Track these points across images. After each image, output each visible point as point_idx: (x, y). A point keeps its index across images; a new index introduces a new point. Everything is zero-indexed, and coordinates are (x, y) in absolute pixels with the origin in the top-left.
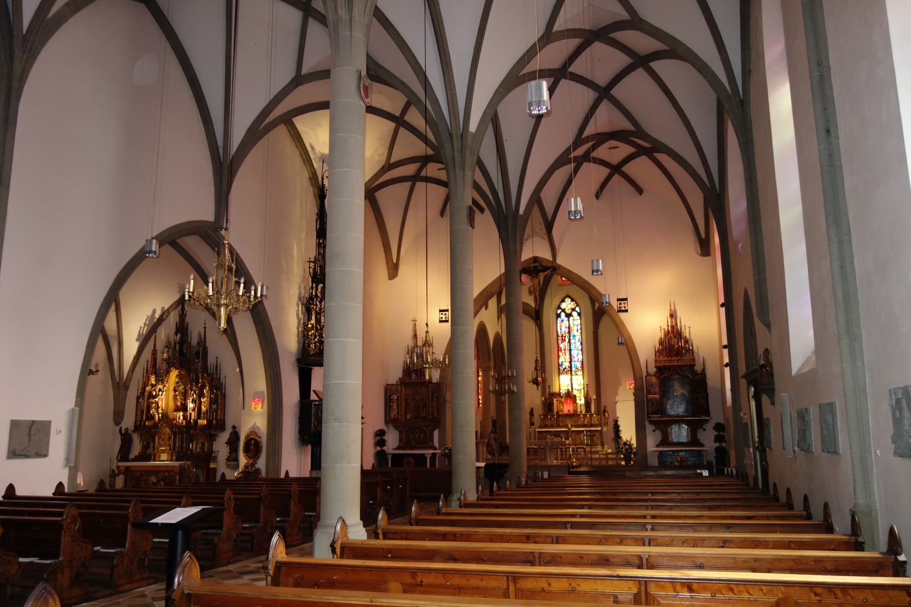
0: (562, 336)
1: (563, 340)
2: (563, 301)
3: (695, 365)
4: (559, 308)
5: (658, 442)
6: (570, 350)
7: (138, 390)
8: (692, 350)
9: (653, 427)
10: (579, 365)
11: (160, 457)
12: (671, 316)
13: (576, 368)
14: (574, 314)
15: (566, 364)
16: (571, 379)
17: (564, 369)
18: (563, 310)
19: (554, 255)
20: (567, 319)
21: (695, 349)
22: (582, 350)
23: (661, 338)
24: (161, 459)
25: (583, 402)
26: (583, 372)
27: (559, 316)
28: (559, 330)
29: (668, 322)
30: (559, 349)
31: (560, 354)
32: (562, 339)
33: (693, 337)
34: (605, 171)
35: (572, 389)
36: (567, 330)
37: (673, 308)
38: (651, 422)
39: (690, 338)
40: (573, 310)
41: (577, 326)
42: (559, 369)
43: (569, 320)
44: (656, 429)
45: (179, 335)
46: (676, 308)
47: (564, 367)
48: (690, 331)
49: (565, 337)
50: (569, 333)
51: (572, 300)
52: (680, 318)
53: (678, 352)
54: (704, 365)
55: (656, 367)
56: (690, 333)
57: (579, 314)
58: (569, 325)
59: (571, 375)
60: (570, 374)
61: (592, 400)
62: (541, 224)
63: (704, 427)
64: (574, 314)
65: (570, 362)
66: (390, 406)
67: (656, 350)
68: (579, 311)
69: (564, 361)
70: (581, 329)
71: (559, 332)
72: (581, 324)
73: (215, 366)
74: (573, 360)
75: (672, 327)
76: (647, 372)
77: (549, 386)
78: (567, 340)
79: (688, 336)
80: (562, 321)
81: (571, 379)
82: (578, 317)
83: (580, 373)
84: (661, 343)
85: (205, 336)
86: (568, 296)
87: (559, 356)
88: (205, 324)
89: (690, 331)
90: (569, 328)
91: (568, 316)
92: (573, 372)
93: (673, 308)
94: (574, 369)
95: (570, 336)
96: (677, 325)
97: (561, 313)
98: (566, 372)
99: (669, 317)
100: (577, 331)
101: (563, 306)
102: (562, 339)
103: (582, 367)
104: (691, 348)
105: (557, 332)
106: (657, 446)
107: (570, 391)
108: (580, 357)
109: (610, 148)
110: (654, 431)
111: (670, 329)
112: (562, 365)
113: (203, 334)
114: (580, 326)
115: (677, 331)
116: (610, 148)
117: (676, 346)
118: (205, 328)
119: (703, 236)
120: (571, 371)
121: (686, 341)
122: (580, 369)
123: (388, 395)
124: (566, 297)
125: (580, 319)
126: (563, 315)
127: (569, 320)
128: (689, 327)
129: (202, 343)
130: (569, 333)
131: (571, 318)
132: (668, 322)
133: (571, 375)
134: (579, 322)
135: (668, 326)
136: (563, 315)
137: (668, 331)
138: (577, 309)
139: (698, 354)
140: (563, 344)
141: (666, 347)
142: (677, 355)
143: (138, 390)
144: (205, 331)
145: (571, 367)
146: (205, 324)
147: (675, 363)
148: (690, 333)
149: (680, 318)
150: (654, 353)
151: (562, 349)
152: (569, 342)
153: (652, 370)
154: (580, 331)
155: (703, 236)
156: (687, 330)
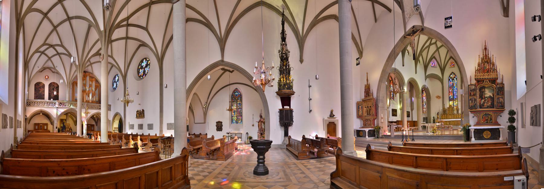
2: (451, 74)
6: (453, 92)
16: (453, 102)
18: (451, 78)
58: (453, 83)
59: (453, 101)
65: (453, 97)
66: (359, 111)
81: (453, 102)
91: (453, 80)
101: (451, 76)
126: (451, 79)
133: (453, 101)
136: (451, 79)
142: (488, 72)
145: (453, 98)
152: (453, 88)
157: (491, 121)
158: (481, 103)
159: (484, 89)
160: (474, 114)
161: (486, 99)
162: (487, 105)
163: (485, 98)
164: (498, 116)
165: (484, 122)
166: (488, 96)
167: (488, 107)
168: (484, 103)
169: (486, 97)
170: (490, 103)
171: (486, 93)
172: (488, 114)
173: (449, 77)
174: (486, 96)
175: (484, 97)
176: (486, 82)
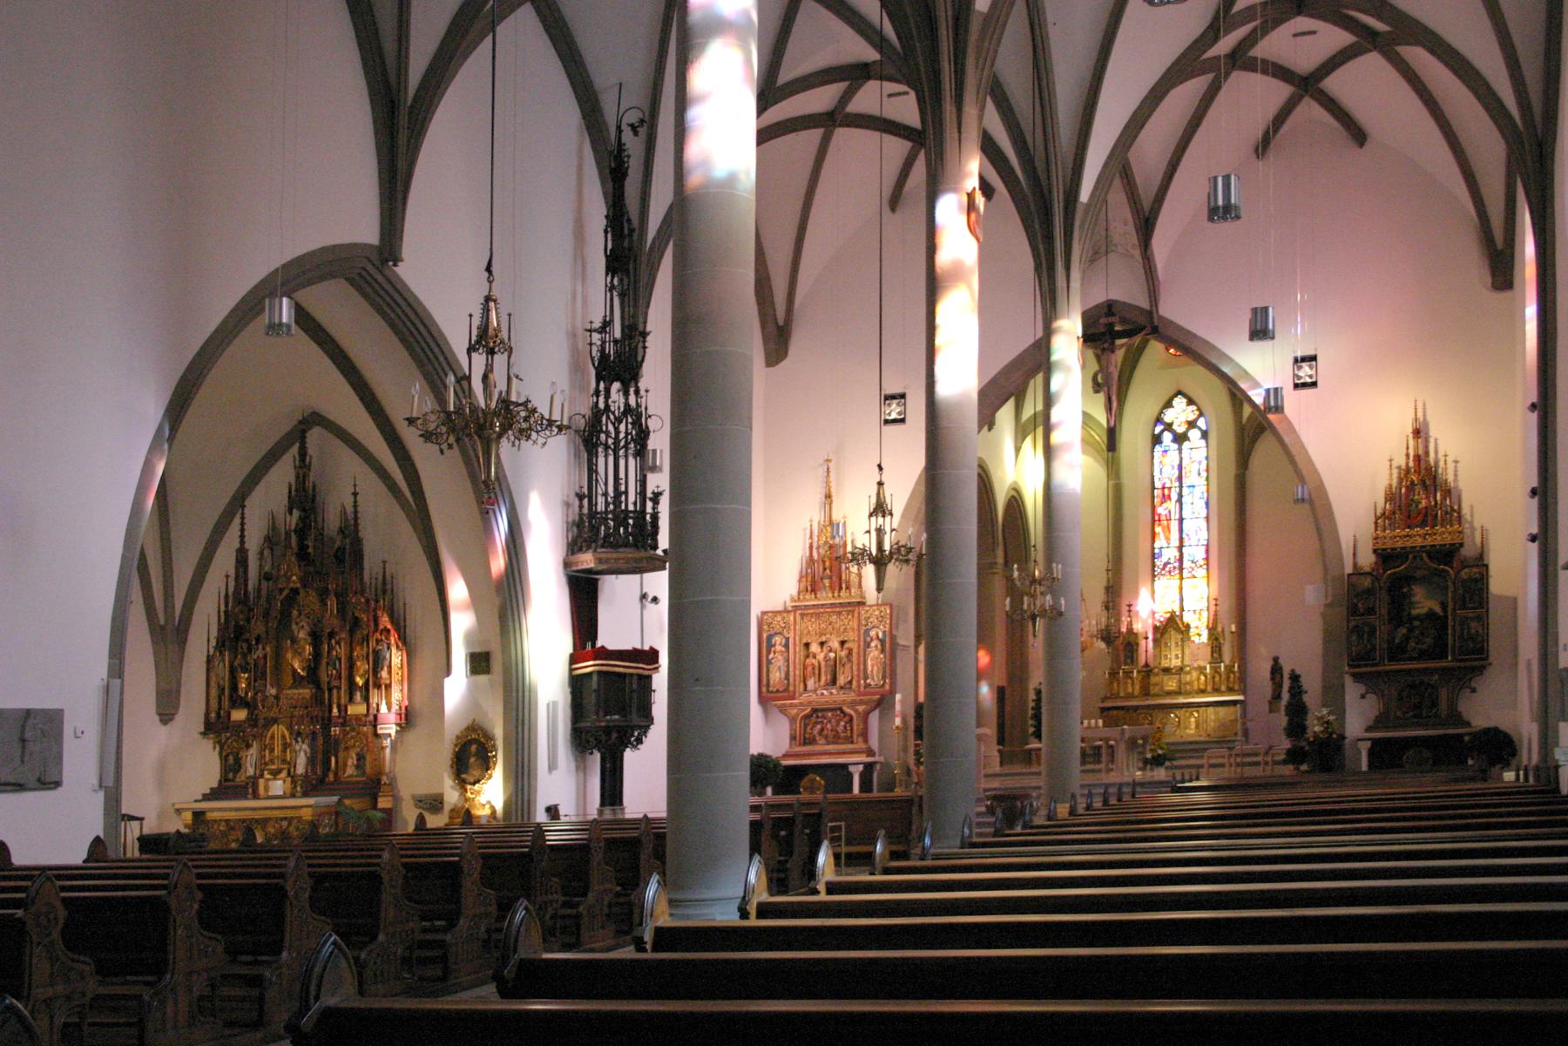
0: (1164, 488)
1: (1165, 498)
3: (1462, 545)
4: (1159, 420)
5: (1371, 723)
7: (208, 641)
8: (1459, 512)
9: (1361, 688)
10: (1200, 554)
11: (267, 789)
12: (1417, 433)
13: (1193, 562)
14: (1194, 434)
15: (1170, 554)
16: (1181, 588)
17: (1166, 564)
18: (1169, 427)
19: (1153, 293)
20: (1175, 446)
21: (1466, 510)
22: (1207, 518)
23: (1391, 486)
24: (270, 794)
25: (1205, 638)
26: (1208, 569)
27: (1157, 440)
28: (1156, 474)
29: (1408, 448)
30: (1155, 519)
31: (1158, 529)
32: (1164, 495)
33: (1461, 485)
34: (1280, 92)
35: (1182, 609)
36: (1176, 473)
37: (1420, 415)
38: (1357, 677)
39: (1456, 487)
40: (1192, 424)
41: (1200, 462)
42: (1154, 565)
43: (1180, 450)
44: (1366, 693)
45: (296, 513)
46: (1428, 418)
47: (1164, 559)
48: (1456, 471)
49: (1170, 488)
50: (1180, 478)
51: (1191, 402)
52: (1436, 440)
53: (1426, 515)
54: (1483, 547)
55: (1375, 551)
56: (1456, 475)
57: (1205, 435)
58: (1181, 459)
59: (1182, 578)
60: (1178, 576)
61: (1227, 633)
62: (1126, 224)
63: (1473, 684)
64: (1194, 434)
67: (1378, 514)
68: (1204, 428)
69: (1165, 545)
70: (1207, 470)
71: (1156, 480)
72: (1207, 458)
73: (380, 578)
74: (1186, 542)
75: (1418, 458)
76: (1355, 565)
77: (1130, 606)
78: (1174, 496)
79: (1450, 478)
80: (1165, 451)
81: (1181, 588)
82: (1203, 443)
83: (1202, 572)
84: (1390, 497)
85: (356, 512)
86: (1179, 393)
87: (1154, 535)
88: (355, 486)
89: (1456, 471)
90: (1180, 467)
91: (1180, 439)
92: (1185, 572)
93: (1420, 415)
94: (1186, 564)
95: (1181, 487)
96: (1427, 453)
97: (1162, 432)
98: (1170, 572)
99: (1411, 436)
100: (1199, 474)
101: (1168, 416)
102: (1164, 495)
103: (1207, 559)
104: (1456, 507)
105: (1153, 477)
106: (1369, 729)
107: (1178, 613)
108: (1204, 535)
109: (1295, 35)
110: (1363, 697)
111: (1411, 464)
112: (1160, 555)
113: (350, 509)
114: (1205, 463)
115: (1428, 469)
116: (1295, 35)
117: (1424, 501)
118: (355, 494)
119: (1500, 243)
120: (1181, 569)
121: (1448, 492)
122: (1202, 562)
123: (765, 636)
124: (1176, 395)
125: (1207, 447)
126: (1167, 437)
127: (1180, 450)
128: (1456, 462)
129: (351, 529)
130: (1180, 478)
131: (1186, 445)
132: (1408, 448)
133: (1182, 578)
134: (1203, 453)
135: (1408, 455)
136: (1167, 437)
137: (1408, 470)
138: (1201, 423)
139: (1471, 523)
140: (1164, 505)
141: (1400, 506)
142: (1423, 524)
143: (208, 641)
144: (355, 502)
145: (1181, 560)
146: (355, 486)
147: (1419, 542)
148: (1456, 475)
149: (1436, 440)
150: (1373, 520)
151: (1163, 518)
153: (1367, 559)
154: (1204, 474)
155: (1500, 243)
156: (1451, 466)
157: (1434, 711)
158: (1397, 641)
159: (1409, 585)
160: (1366, 685)
161: (1416, 623)
162: (1420, 646)
163: (1411, 619)
164: (1461, 688)
165: (1404, 713)
166: (1424, 611)
167: (1423, 655)
168: (1407, 638)
169: (1418, 617)
170: (1429, 641)
171: (1414, 599)
172: (1422, 683)
173: (1159, 420)
174: (1414, 612)
175: (1405, 619)
176: (1418, 559)
